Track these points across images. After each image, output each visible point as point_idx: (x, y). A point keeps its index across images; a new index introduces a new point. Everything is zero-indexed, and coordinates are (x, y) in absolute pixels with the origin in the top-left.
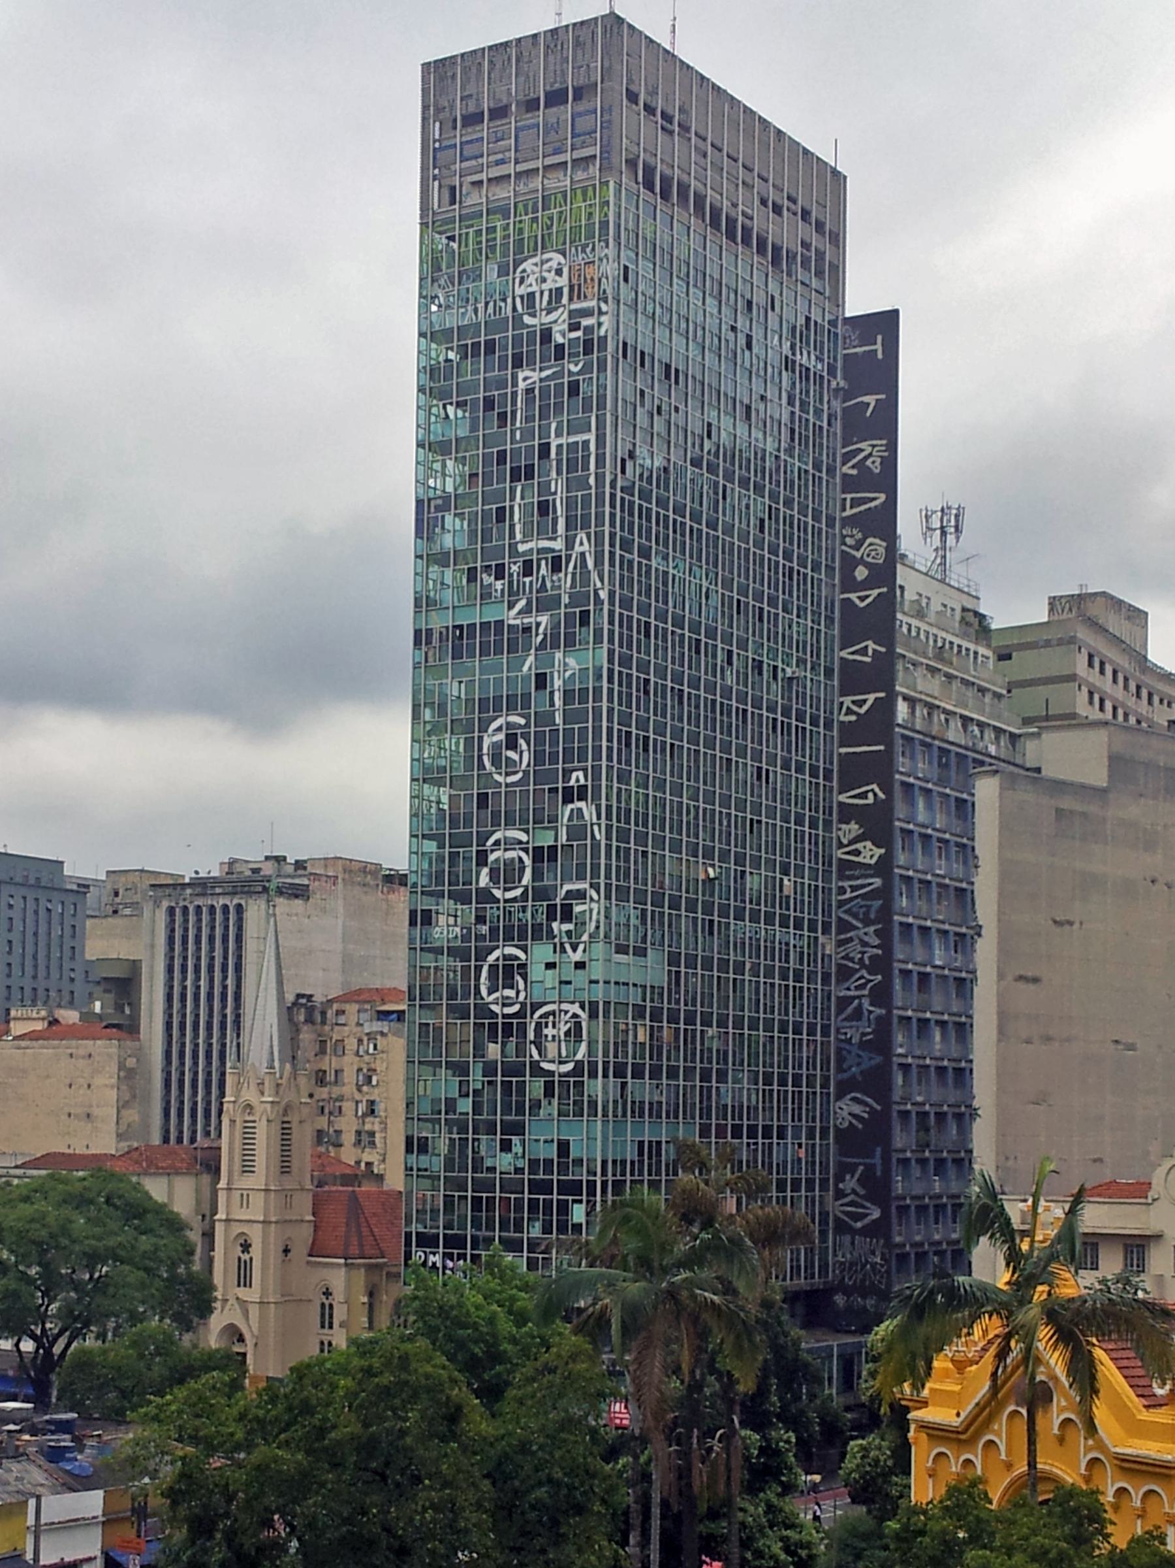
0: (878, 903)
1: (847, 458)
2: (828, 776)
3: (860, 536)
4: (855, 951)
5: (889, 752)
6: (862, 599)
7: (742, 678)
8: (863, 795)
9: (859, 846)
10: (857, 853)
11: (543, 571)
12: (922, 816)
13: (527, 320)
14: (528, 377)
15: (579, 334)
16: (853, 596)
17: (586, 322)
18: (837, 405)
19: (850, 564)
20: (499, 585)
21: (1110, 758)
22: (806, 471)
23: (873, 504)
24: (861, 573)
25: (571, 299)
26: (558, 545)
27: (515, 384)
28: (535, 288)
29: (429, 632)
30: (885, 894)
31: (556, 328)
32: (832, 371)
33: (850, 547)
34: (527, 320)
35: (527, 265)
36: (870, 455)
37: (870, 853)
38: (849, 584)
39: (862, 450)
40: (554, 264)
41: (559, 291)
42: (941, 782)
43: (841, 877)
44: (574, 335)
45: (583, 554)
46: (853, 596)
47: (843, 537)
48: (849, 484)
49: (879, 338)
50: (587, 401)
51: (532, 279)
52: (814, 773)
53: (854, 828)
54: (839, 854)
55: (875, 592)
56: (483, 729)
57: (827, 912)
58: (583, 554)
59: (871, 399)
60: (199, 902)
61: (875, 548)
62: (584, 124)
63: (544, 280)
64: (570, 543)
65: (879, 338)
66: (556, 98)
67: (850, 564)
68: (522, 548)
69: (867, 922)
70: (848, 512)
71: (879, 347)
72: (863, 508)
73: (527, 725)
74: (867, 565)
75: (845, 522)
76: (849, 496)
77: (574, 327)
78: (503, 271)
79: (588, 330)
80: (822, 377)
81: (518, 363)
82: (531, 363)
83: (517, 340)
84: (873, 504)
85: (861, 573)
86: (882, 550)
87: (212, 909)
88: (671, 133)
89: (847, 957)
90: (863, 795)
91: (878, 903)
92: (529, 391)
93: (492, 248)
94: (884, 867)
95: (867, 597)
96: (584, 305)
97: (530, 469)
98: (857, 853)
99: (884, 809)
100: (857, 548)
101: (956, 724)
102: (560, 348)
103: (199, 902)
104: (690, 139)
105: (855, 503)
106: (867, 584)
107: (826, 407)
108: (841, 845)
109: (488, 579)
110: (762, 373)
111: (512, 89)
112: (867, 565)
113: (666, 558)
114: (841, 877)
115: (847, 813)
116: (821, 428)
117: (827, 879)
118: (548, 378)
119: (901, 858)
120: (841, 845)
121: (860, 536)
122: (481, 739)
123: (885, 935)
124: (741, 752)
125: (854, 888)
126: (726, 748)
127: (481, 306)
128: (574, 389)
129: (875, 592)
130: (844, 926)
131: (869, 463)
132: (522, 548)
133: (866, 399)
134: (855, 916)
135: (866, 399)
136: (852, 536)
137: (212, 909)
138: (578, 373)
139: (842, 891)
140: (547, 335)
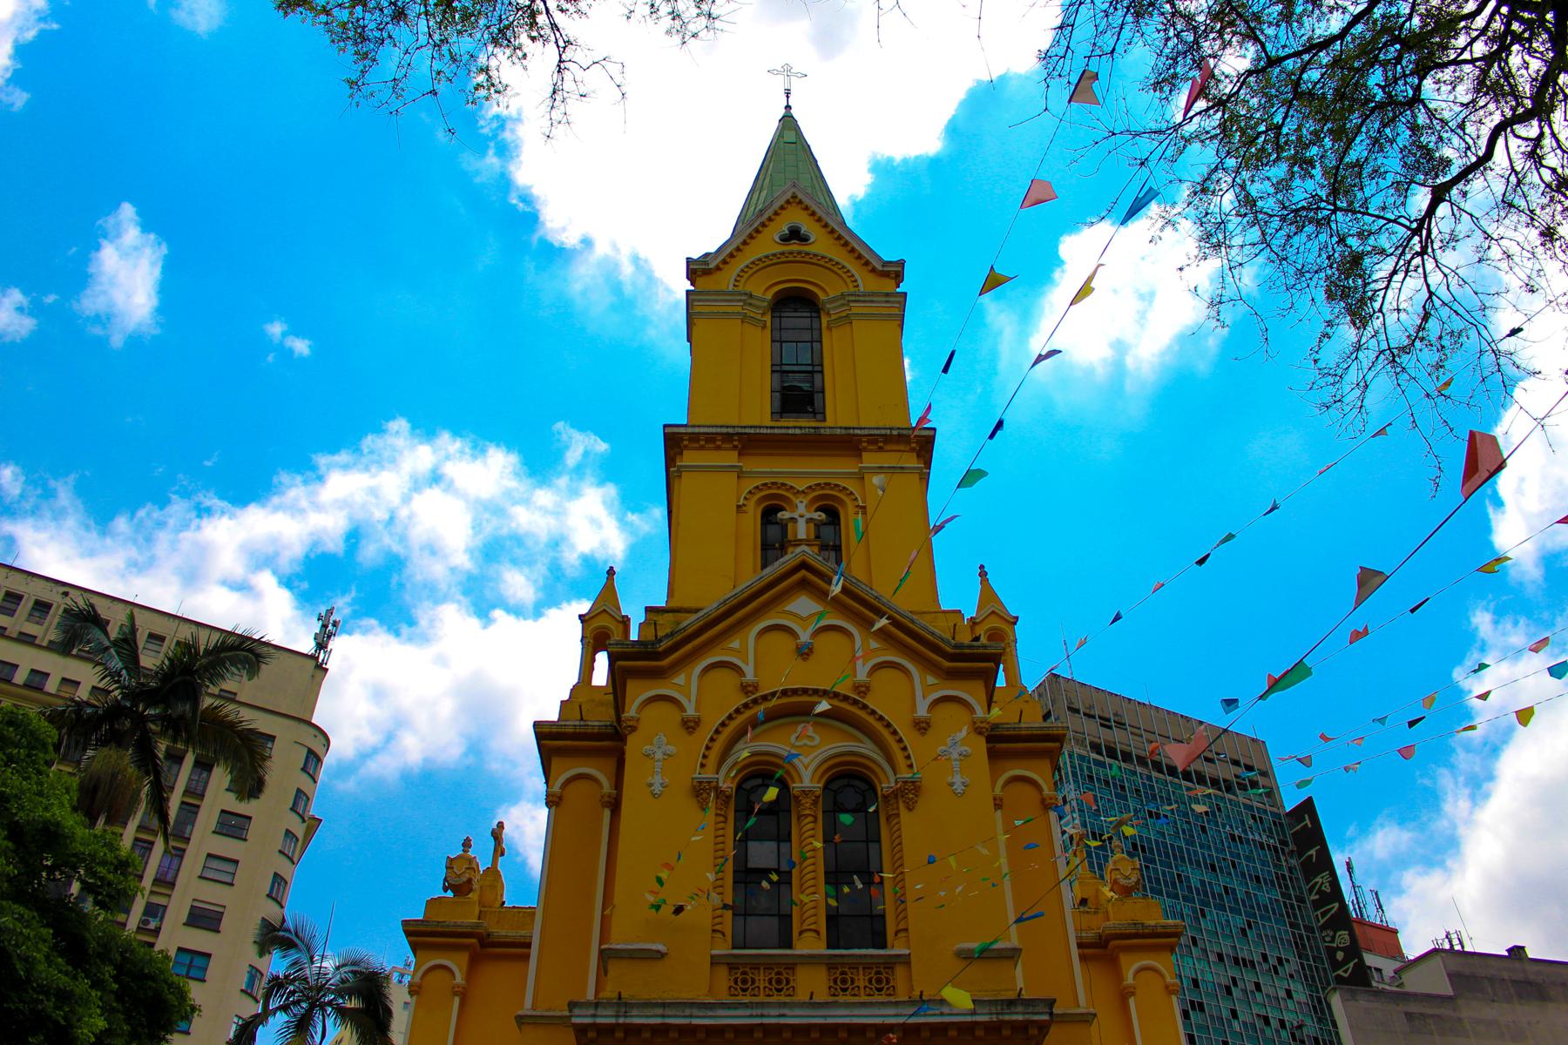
1: (1311, 890)
3: (1331, 933)
6: (1345, 971)
16: (1340, 972)
18: (1293, 862)
19: (1331, 952)
21: (1449, 975)
22: (1277, 900)
23: (1333, 911)
24: (1340, 956)
32: (1284, 843)
33: (1330, 942)
36: (1323, 883)
38: (1336, 965)
39: (1316, 883)
46: (1340, 972)
47: (1323, 937)
48: (1317, 905)
49: (1306, 816)
55: (1351, 964)
59: (1313, 852)
61: (1343, 937)
65: (1306, 816)
67: (1331, 952)
70: (1322, 922)
71: (1308, 821)
72: (1328, 916)
74: (1342, 949)
75: (1323, 928)
76: (1318, 913)
80: (1275, 848)
84: (1333, 911)
85: (1340, 956)
86: (1347, 937)
88: (1110, 727)
95: (1348, 969)
100: (1333, 941)
105: (1323, 914)
106: (1346, 961)
107: (1284, 864)
110: (1220, 846)
112: (1342, 949)
116: (1283, 876)
121: (1331, 933)
129: (1351, 964)
131: (1323, 888)
133: (1310, 853)
135: (1310, 853)
136: (1328, 935)
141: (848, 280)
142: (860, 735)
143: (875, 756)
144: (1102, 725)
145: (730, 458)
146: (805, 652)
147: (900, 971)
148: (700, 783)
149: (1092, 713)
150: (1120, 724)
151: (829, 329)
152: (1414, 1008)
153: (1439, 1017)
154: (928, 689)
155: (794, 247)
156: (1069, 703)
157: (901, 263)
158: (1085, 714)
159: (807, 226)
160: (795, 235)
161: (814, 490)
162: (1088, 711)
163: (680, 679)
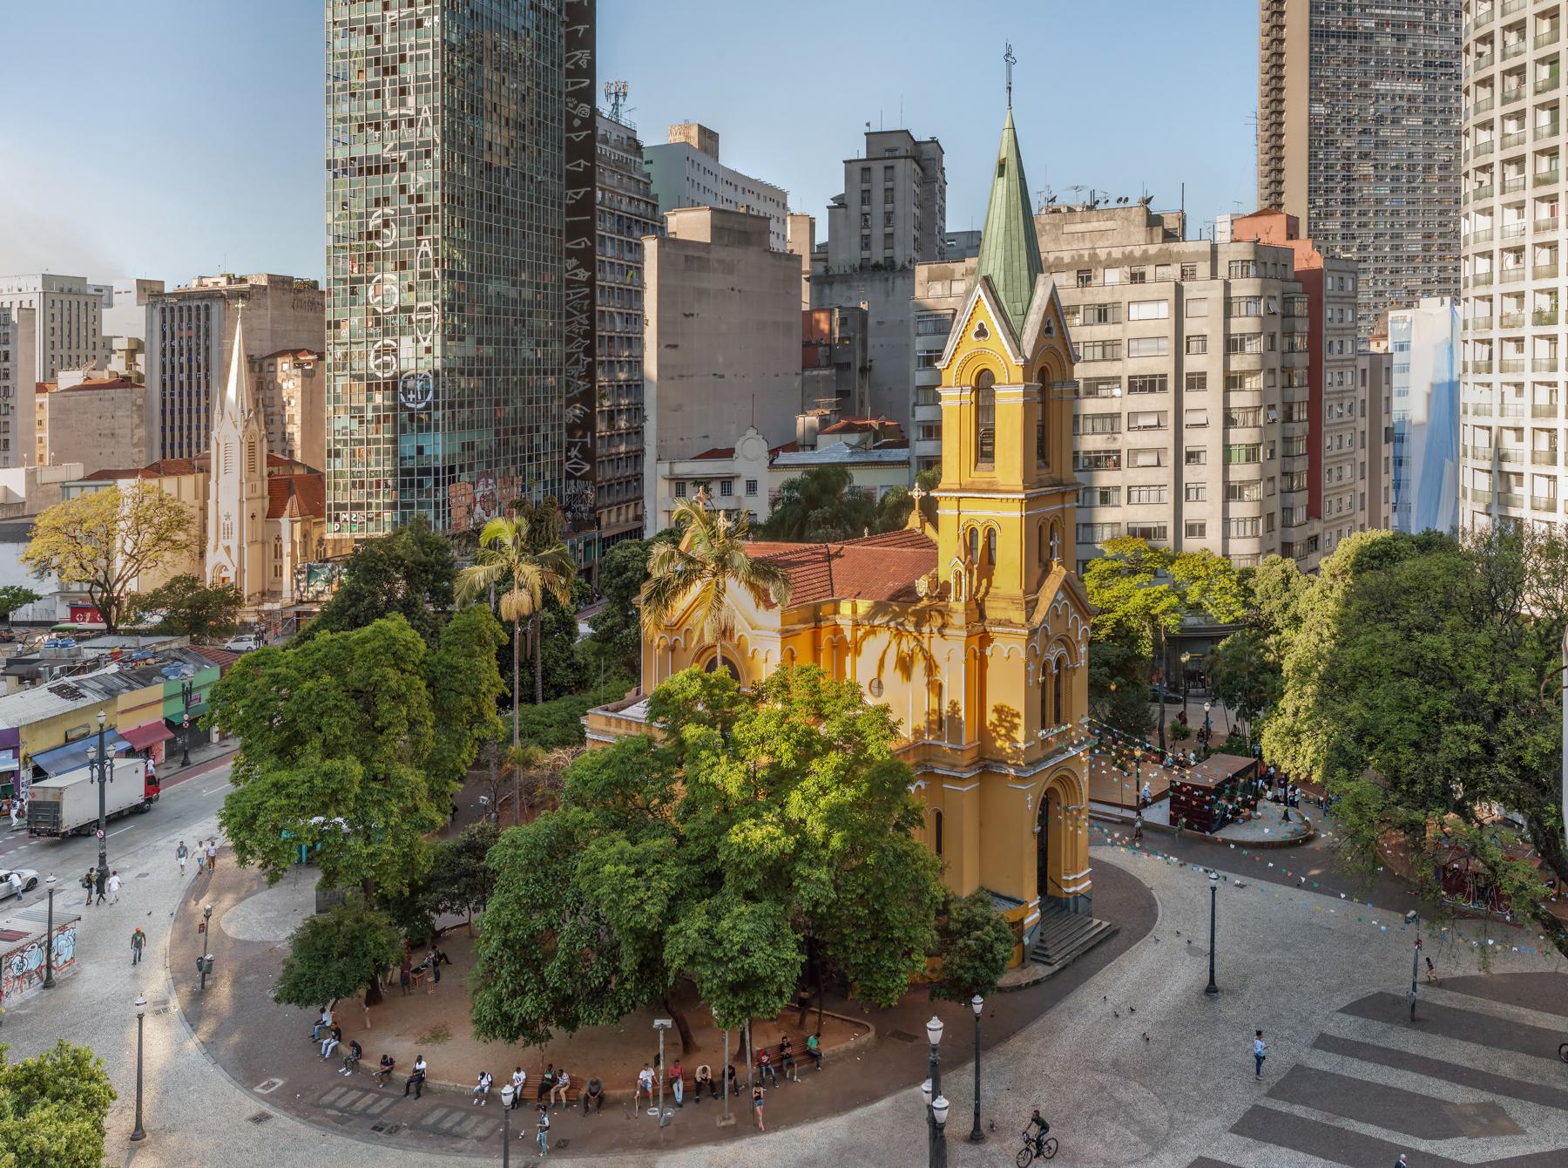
0: (587, 302)
2: (560, 235)
4: (576, 329)
5: (593, 220)
7: (514, 184)
8: (579, 244)
9: (577, 271)
10: (576, 275)
11: (403, 127)
12: (609, 252)
20: (377, 134)
26: (412, 112)
29: (335, 161)
30: (592, 296)
37: (583, 275)
42: (620, 232)
43: (568, 288)
45: (426, 119)
52: (553, 233)
53: (574, 262)
54: (566, 276)
56: (369, 215)
57: (560, 306)
58: (426, 119)
60: (182, 304)
64: (418, 111)
68: (390, 113)
69: (582, 312)
73: (395, 215)
87: (189, 308)
89: (571, 331)
90: (579, 244)
91: (587, 302)
94: (591, 282)
97: (394, 69)
98: (576, 275)
99: (591, 251)
101: (625, 201)
103: (182, 304)
108: (567, 271)
109: (371, 131)
113: (472, 119)
114: (568, 288)
115: (571, 254)
117: (560, 289)
119: (599, 276)
120: (567, 271)
122: (367, 223)
123: (591, 319)
124: (514, 224)
125: (574, 294)
126: (506, 223)
130: (569, 315)
132: (390, 113)
134: (575, 309)
137: (189, 308)
139: (568, 295)
152: (690, 252)
153: (699, 258)
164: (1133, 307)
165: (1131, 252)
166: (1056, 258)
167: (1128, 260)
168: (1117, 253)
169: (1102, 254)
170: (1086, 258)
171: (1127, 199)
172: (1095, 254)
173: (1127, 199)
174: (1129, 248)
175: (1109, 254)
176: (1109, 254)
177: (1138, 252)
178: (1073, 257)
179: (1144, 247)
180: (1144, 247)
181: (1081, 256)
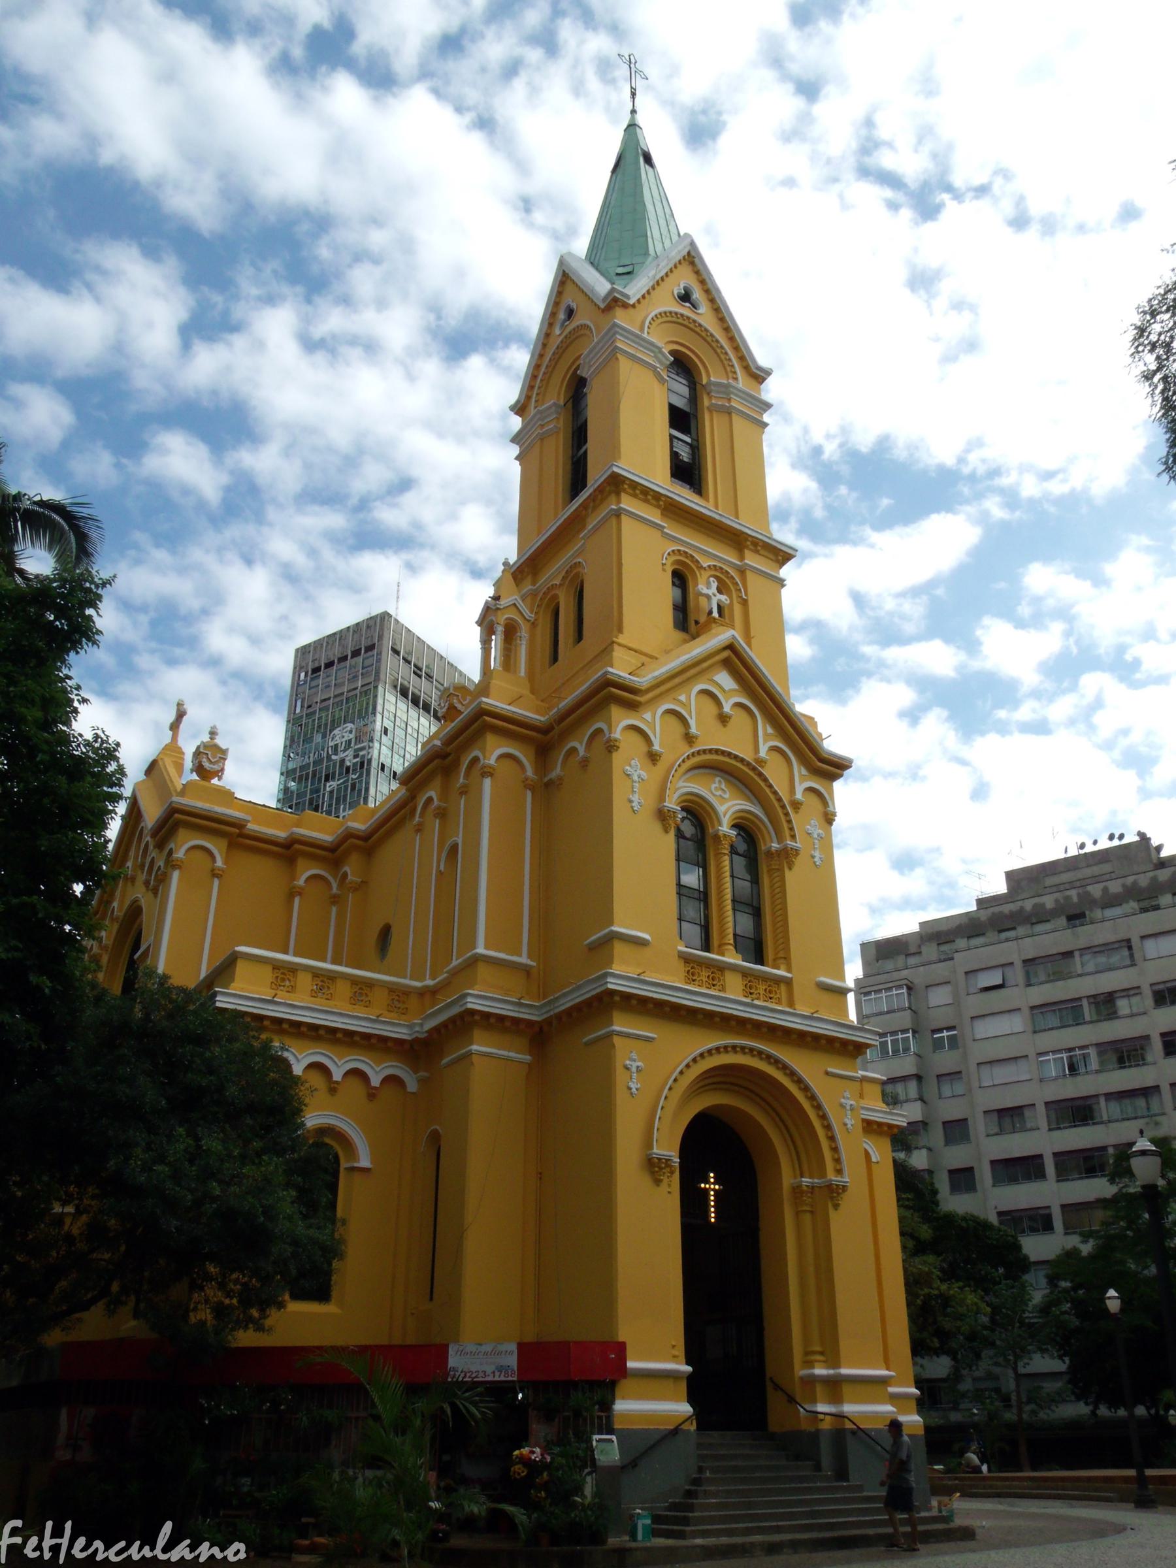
13: (334, 757)
14: (332, 785)
15: (358, 759)
17: (361, 753)
25: (355, 744)
27: (325, 789)
28: (339, 741)
31: (347, 759)
34: (334, 757)
35: (336, 732)
40: (349, 729)
41: (350, 741)
44: (355, 760)
50: (360, 791)
51: (337, 738)
62: (367, 663)
63: (343, 737)
66: (356, 653)
77: (356, 756)
78: (324, 736)
79: (363, 756)
81: (327, 780)
82: (333, 779)
83: (328, 767)
88: (420, 677)
92: (331, 792)
93: (319, 727)
96: (362, 745)
102: (348, 769)
104: (432, 682)
111: (336, 653)
118: (341, 784)
127: (312, 755)
128: (353, 786)
138: (356, 779)
140: (342, 761)
141: (728, 369)
142: (756, 801)
143: (760, 814)
144: (414, 672)
145: (654, 515)
146: (723, 719)
147: (783, 987)
148: (669, 811)
149: (409, 659)
150: (429, 677)
151: (710, 411)
154: (802, 780)
155: (685, 310)
156: (394, 643)
157: (768, 373)
158: (404, 658)
159: (697, 294)
160: (685, 297)
161: (681, 555)
162: (406, 656)
163: (648, 716)
164: (1150, 944)
165: (1135, 883)
166: (1035, 906)
167: (1132, 893)
168: (1115, 887)
169: (1096, 890)
170: (1075, 899)
171: (1121, 837)
172: (1088, 894)
173: (1121, 837)
174: (1130, 880)
175: (1105, 890)
176: (1105, 890)
177: (1144, 881)
178: (1057, 901)
179: (1151, 874)
180: (1151, 874)
181: (1067, 898)
